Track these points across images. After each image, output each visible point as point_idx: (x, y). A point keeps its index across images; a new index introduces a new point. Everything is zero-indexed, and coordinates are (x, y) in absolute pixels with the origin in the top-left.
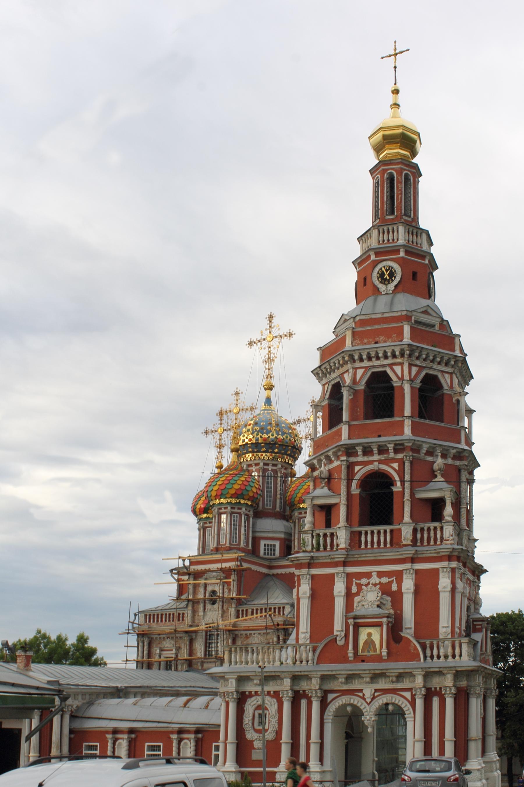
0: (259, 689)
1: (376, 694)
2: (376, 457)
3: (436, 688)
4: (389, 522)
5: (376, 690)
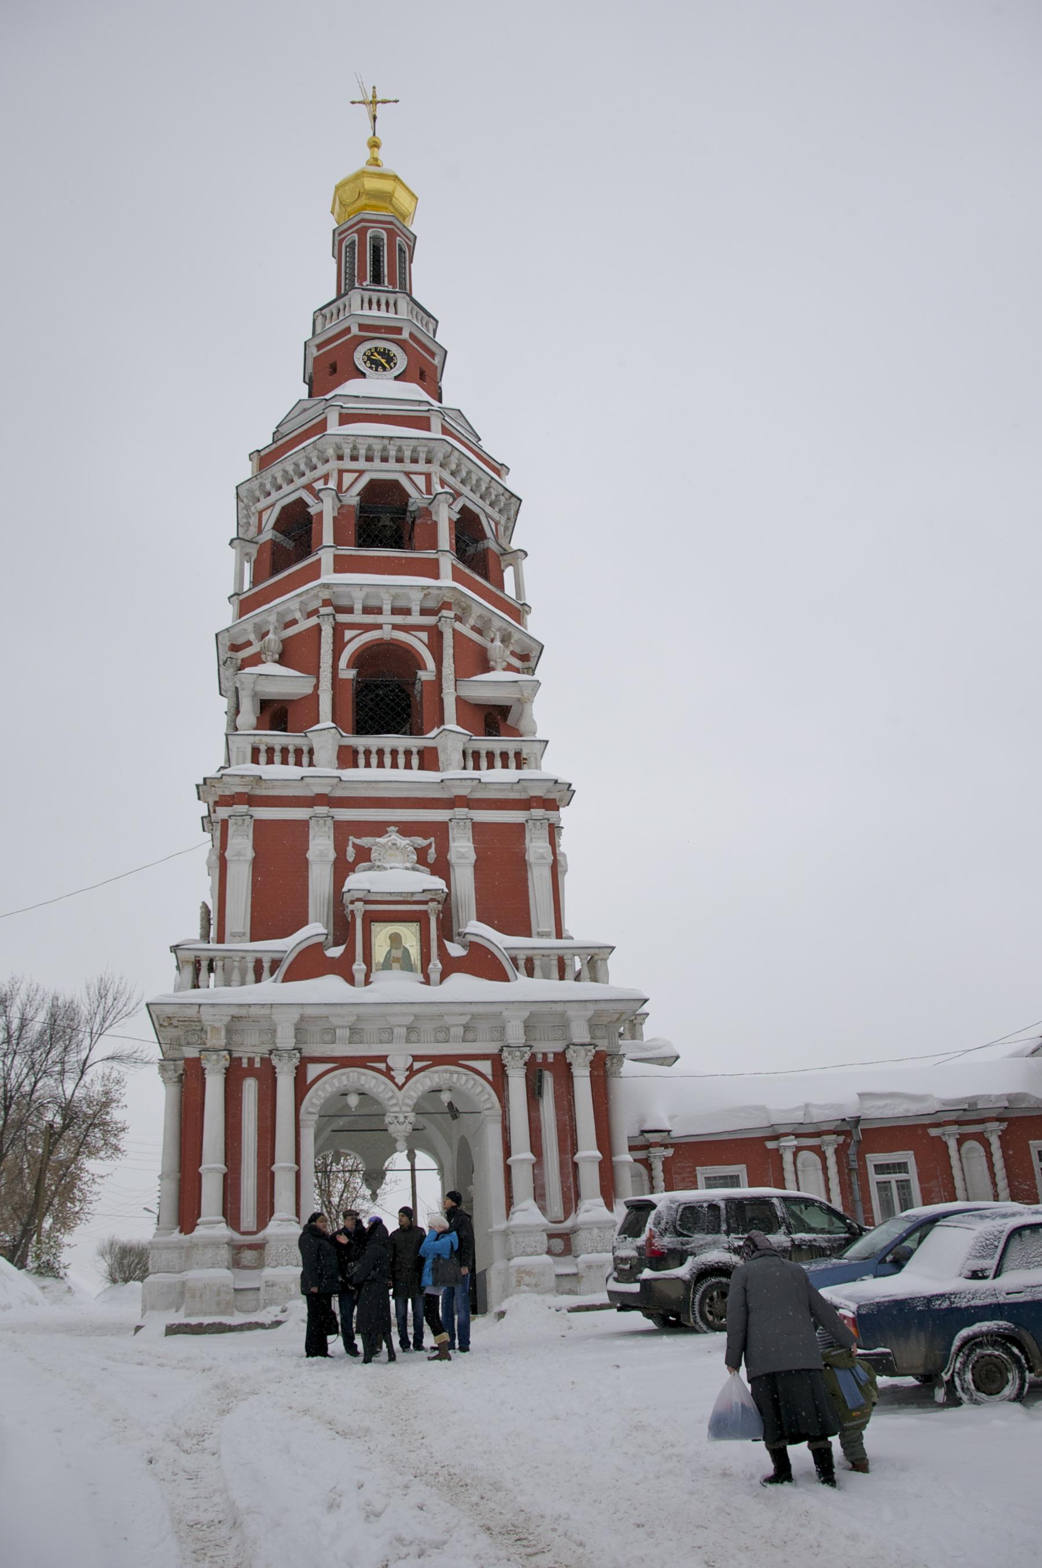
1: (417, 1065)
2: (387, 618)
4: (417, 731)
5: (416, 1058)
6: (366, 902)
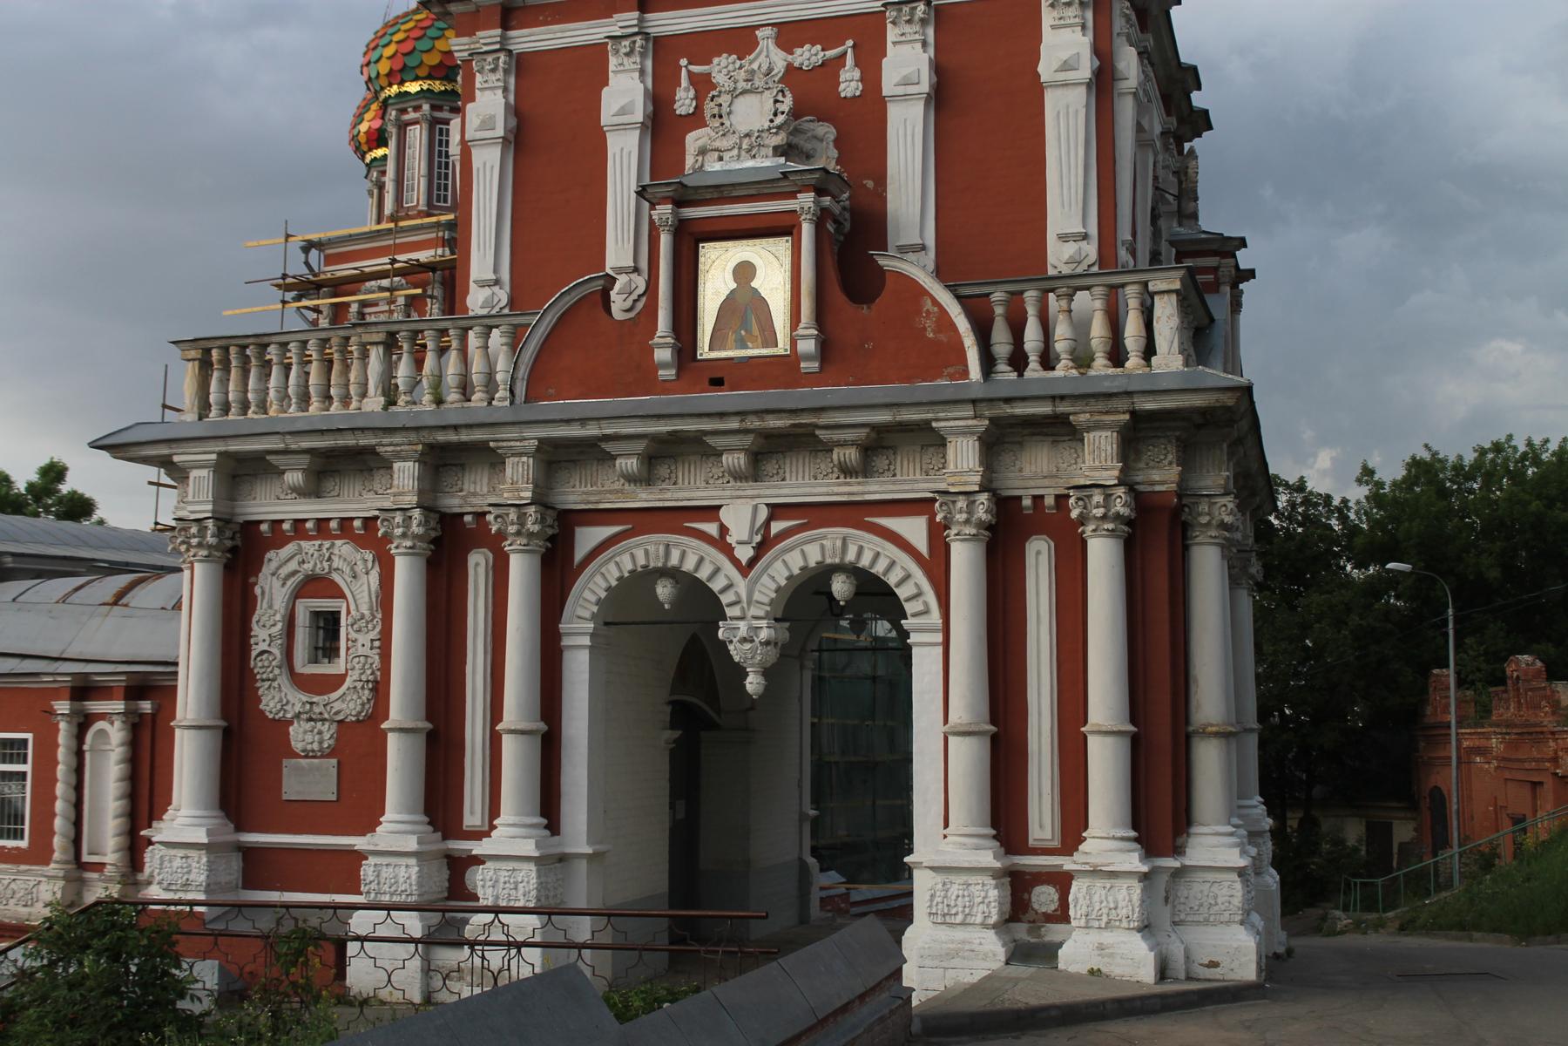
0: (310, 510)
1: (776, 527)
3: (1038, 499)
5: (776, 511)
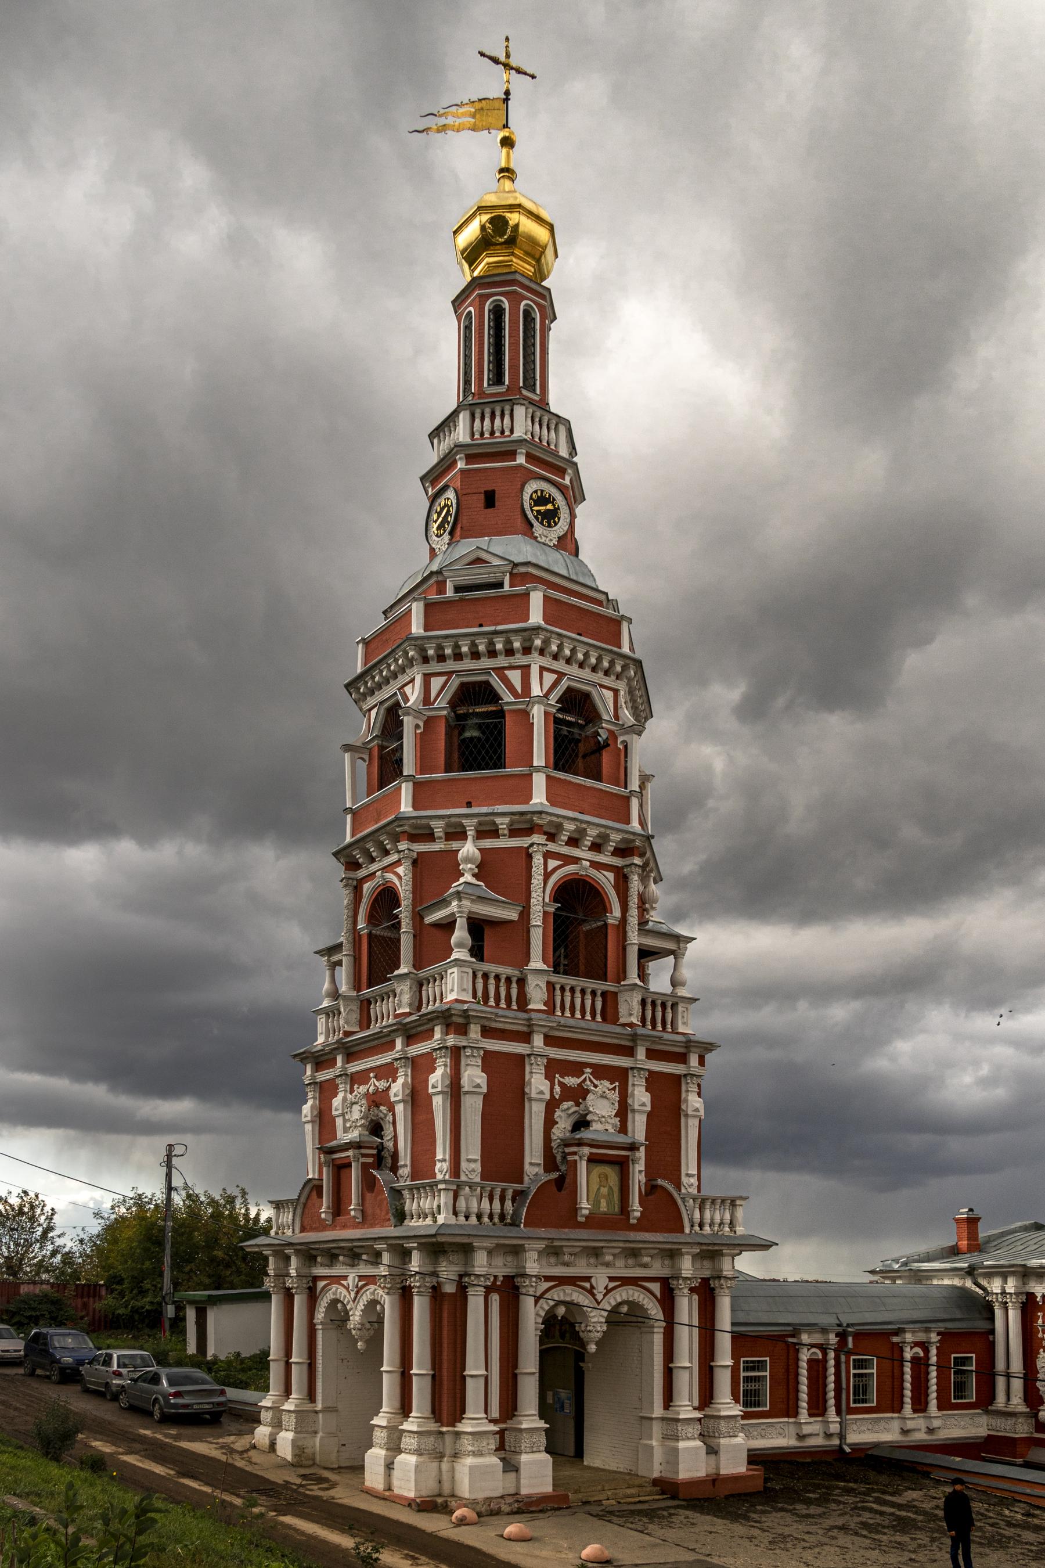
5: (611, 1279)
6: (591, 1146)
